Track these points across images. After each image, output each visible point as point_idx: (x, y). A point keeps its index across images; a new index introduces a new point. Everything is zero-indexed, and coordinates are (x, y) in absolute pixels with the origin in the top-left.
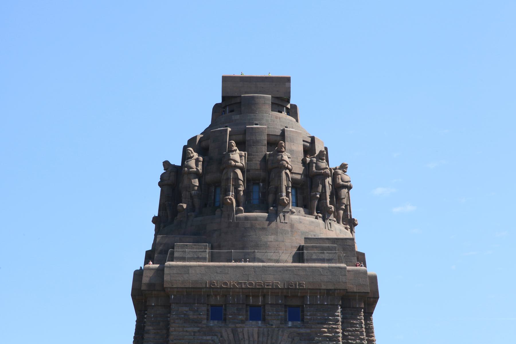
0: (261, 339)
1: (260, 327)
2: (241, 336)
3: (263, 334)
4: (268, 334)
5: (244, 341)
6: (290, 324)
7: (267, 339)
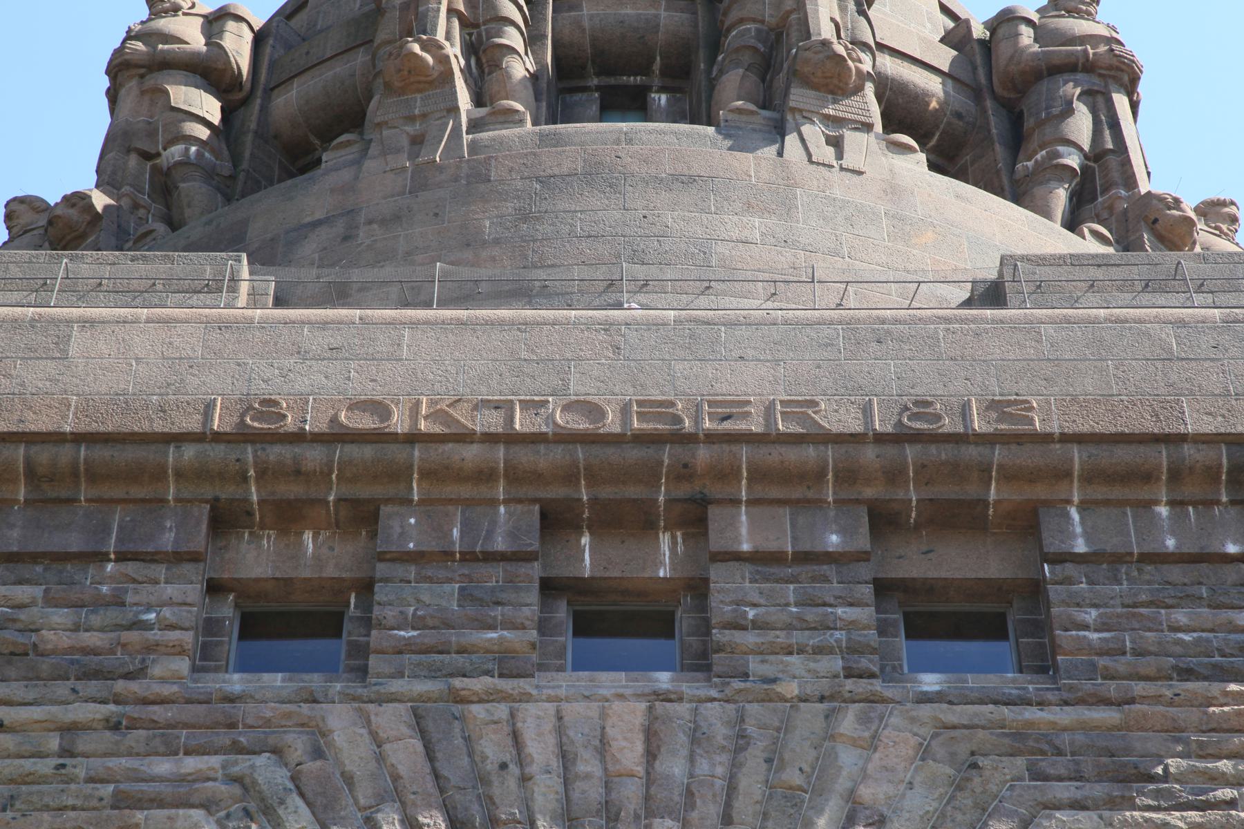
0: (674, 767)
1: (665, 697)
2: (493, 748)
3: (697, 737)
4: (742, 735)
5: (525, 779)
6: (930, 682)
7: (735, 767)
